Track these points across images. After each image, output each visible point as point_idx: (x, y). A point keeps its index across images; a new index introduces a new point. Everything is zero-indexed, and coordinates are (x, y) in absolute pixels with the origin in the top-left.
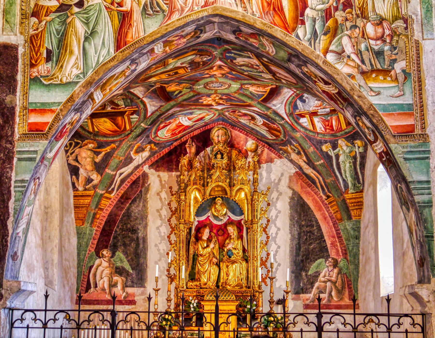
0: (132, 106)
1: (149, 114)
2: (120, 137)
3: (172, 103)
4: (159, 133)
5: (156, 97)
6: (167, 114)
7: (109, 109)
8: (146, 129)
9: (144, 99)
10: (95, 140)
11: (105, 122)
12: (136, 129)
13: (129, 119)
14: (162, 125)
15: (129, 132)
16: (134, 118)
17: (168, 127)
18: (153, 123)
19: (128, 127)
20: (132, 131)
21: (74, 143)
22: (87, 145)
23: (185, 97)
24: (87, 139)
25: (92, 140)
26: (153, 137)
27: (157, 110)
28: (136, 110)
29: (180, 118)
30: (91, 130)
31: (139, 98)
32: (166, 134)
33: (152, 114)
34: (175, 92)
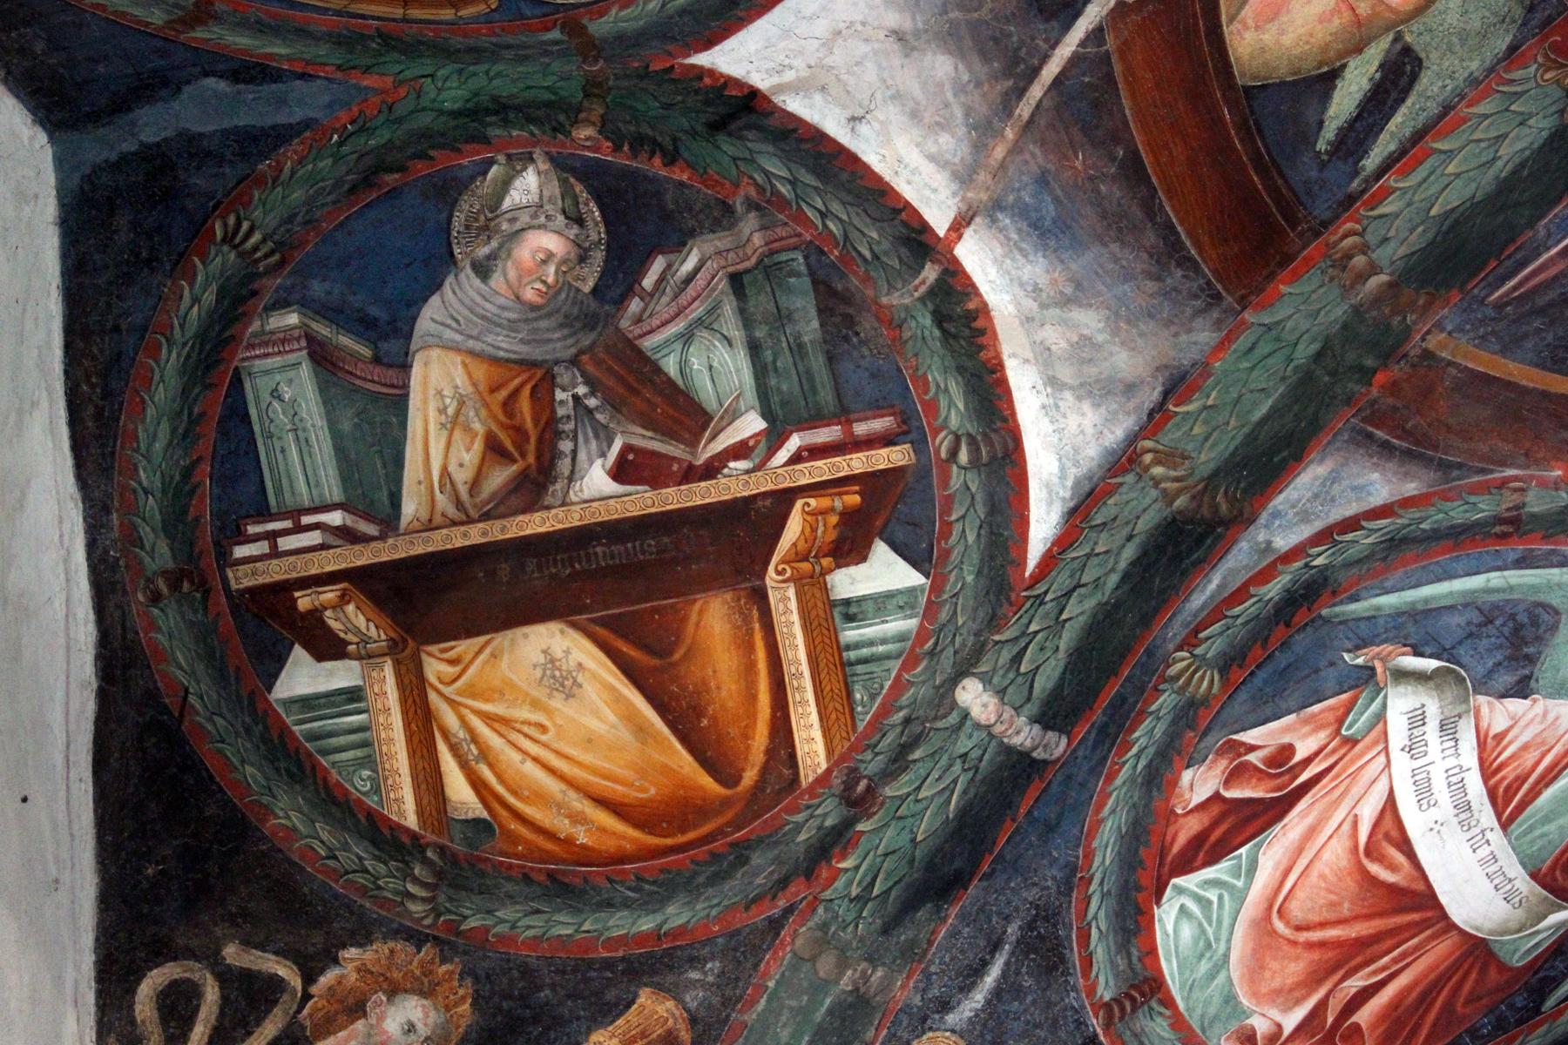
0: (843, 415)
1: (1043, 525)
2: (733, 890)
3: (1305, 308)
4: (1174, 922)
5: (1113, 192)
6: (1239, 558)
7: (594, 486)
8: (1019, 769)
9: (977, 257)
10: (447, 942)
11: (562, 682)
12: (899, 761)
13: (826, 616)
14: (1199, 784)
15: (830, 812)
16: (882, 603)
17: (1271, 852)
18: (1097, 686)
19: (812, 747)
20: (858, 801)
21: (211, 994)
22: (356, 1009)
23: (1454, 178)
24: (361, 936)
25: (417, 938)
26: (1105, 993)
27: (1124, 461)
28: (895, 473)
29: (1400, 703)
30: (406, 809)
31: (918, 241)
32: (1256, 969)
33: (1082, 512)
34: (1326, 80)
